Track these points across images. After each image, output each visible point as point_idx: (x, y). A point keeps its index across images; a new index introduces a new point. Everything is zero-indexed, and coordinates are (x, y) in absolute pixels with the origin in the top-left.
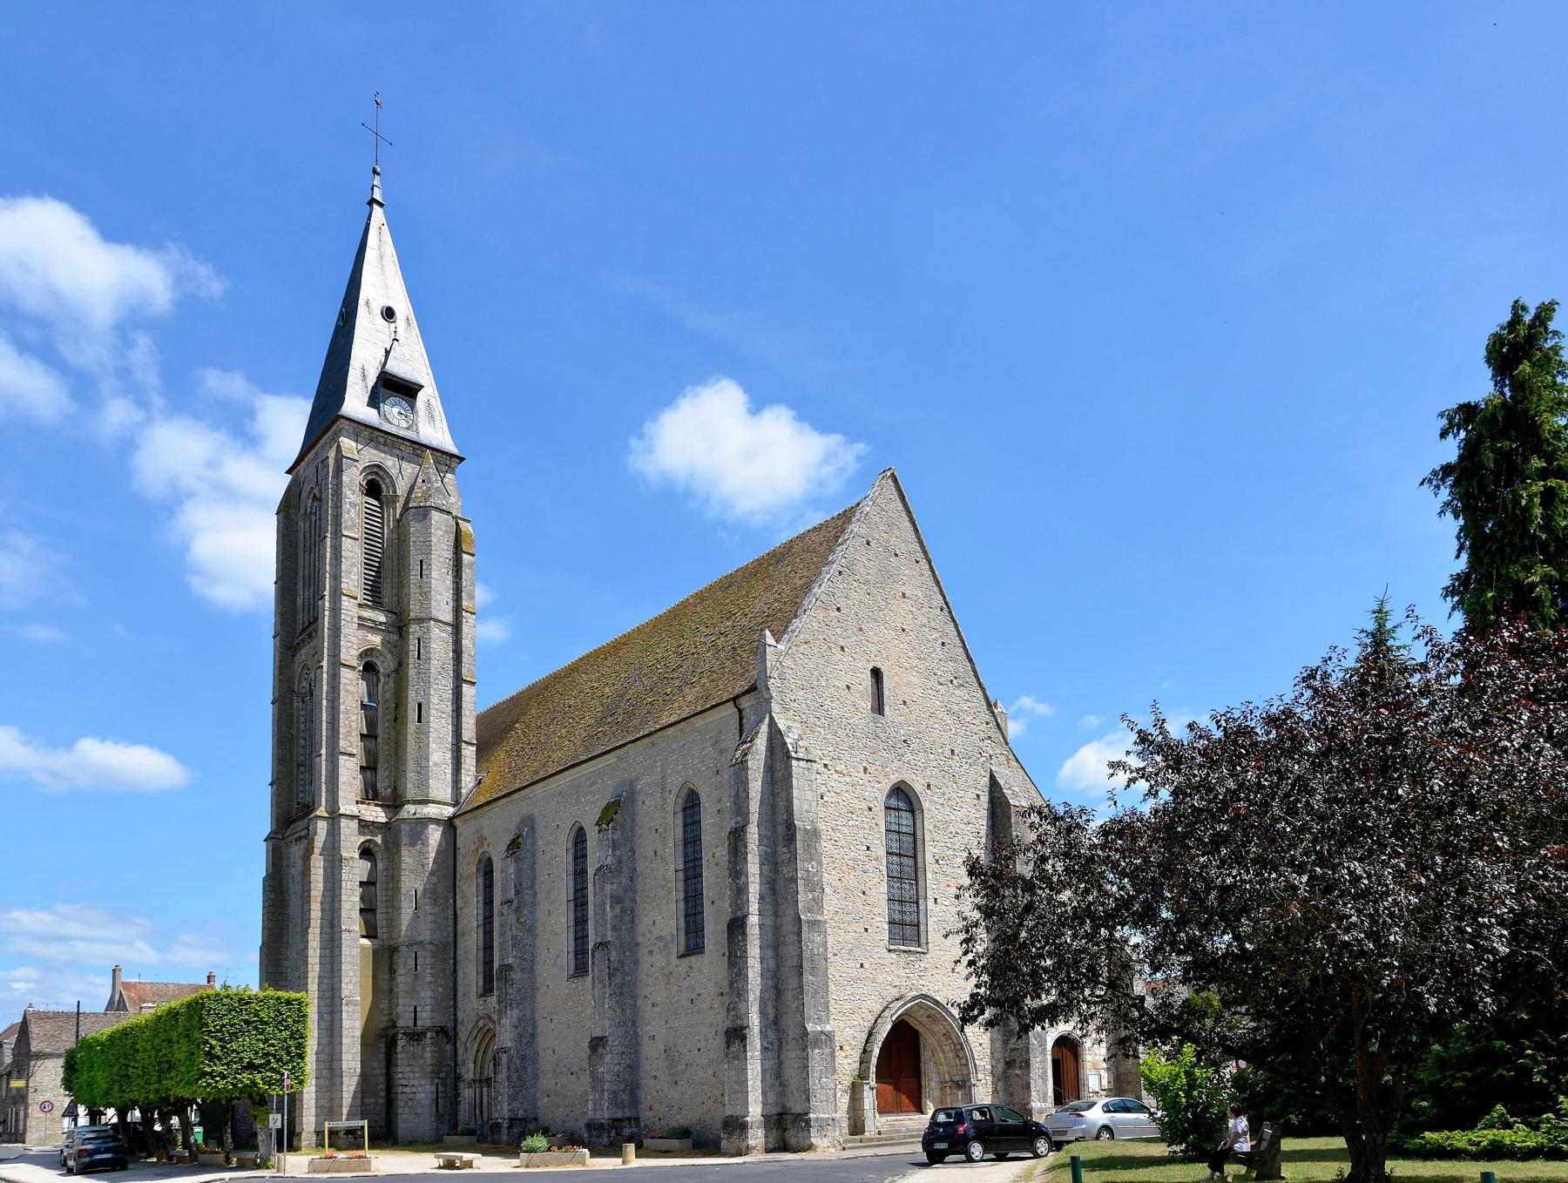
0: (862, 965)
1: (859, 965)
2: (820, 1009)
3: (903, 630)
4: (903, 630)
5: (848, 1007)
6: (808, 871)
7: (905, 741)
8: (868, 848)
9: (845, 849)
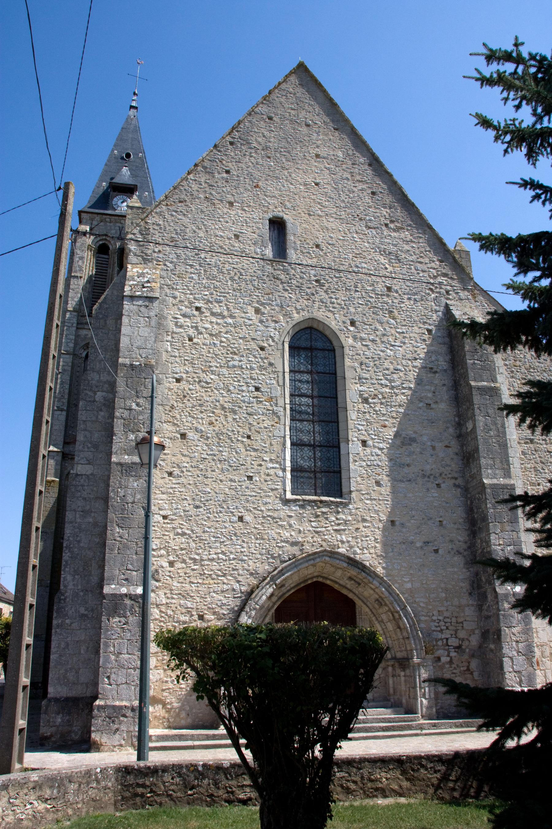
0: (241, 519)
1: (235, 519)
2: (130, 567)
3: (317, 184)
4: (317, 184)
5: (214, 568)
6: (130, 410)
7: (317, 281)
8: (257, 389)
9: (222, 391)
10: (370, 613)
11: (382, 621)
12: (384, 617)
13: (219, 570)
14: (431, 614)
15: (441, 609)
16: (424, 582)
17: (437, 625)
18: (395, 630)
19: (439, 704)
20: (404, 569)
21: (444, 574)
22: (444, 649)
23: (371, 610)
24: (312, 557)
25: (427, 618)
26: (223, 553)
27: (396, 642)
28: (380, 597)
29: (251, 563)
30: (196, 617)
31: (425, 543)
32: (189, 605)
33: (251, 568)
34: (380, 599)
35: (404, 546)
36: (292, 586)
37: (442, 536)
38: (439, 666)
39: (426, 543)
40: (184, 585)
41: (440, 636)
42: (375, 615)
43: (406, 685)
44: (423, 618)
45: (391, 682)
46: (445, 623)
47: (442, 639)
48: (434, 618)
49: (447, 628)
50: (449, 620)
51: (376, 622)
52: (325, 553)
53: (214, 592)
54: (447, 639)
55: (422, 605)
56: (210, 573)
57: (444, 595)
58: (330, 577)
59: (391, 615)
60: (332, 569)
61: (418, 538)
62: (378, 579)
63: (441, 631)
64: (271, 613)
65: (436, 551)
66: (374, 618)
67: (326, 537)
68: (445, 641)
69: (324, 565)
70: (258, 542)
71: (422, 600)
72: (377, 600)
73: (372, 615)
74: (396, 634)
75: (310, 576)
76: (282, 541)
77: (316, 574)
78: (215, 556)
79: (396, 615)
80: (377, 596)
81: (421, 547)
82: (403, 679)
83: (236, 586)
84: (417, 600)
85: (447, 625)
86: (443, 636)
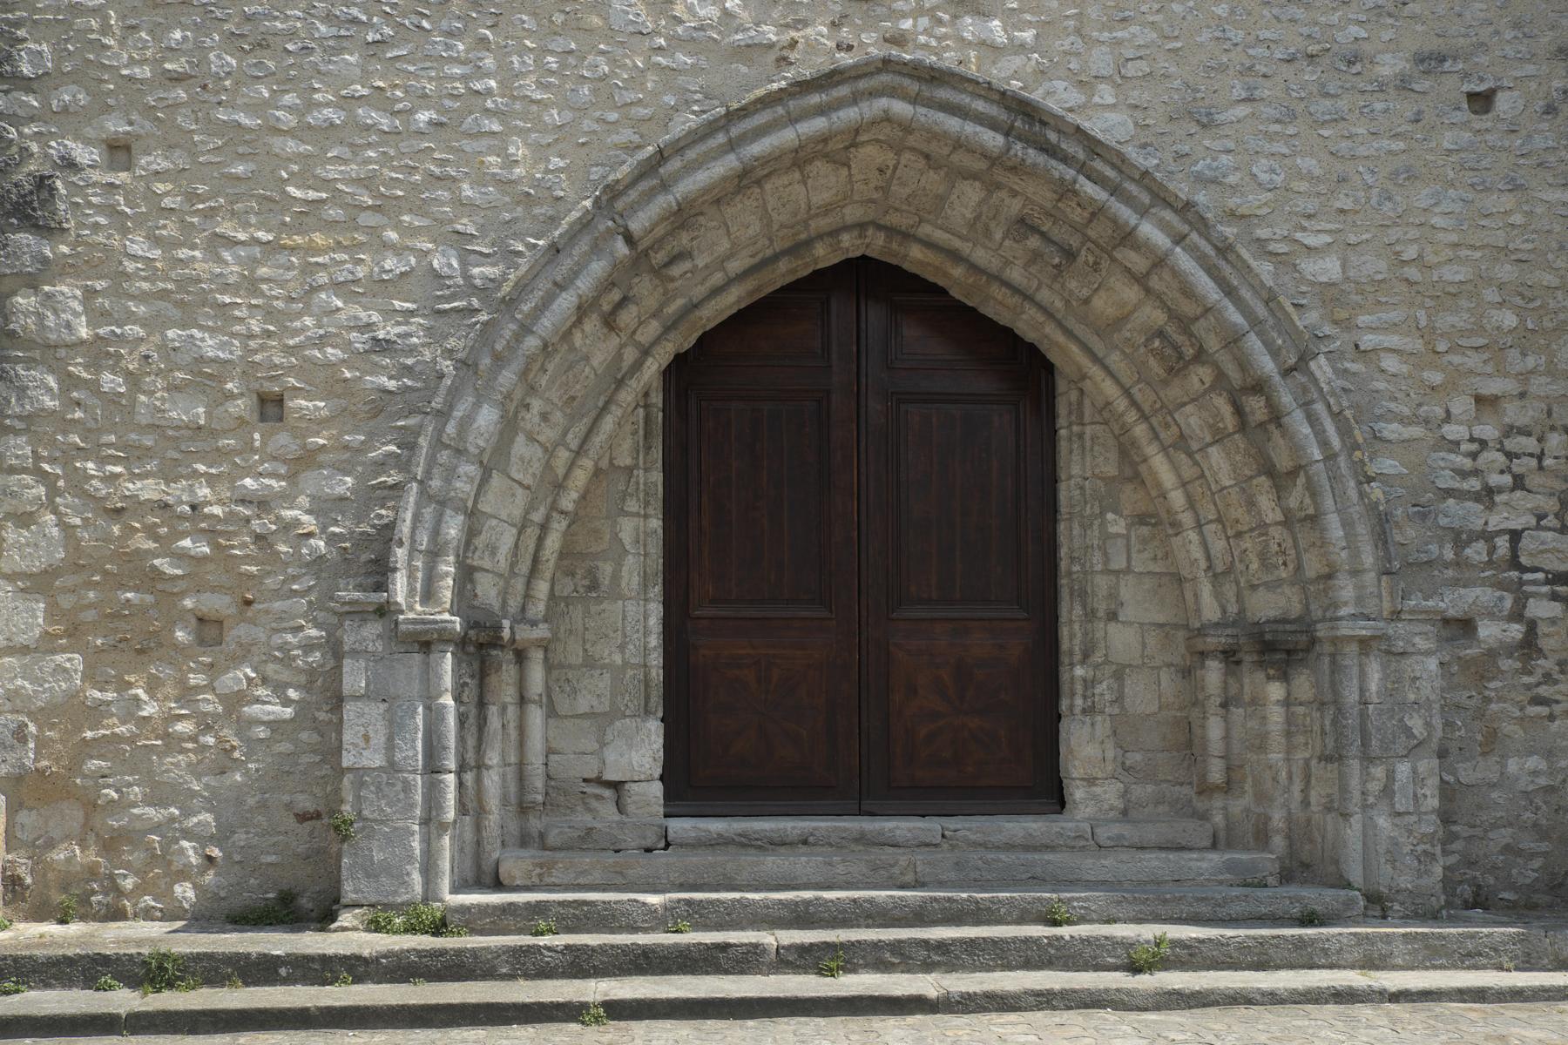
10: (1121, 404)
11: (1182, 443)
12: (1192, 420)
13: (358, 181)
14: (1439, 412)
15: (1492, 387)
16: (1411, 252)
17: (1467, 463)
18: (1244, 483)
19: (1458, 845)
20: (1303, 186)
21: (1517, 219)
22: (1500, 585)
23: (1127, 392)
24: (815, 99)
25: (1416, 431)
26: (379, 99)
27: (1247, 543)
28: (1173, 315)
29: (518, 149)
30: (241, 406)
31: (1420, 59)
32: (210, 346)
33: (519, 171)
34: (1171, 330)
35: (1310, 76)
36: (735, 266)
37: (1516, 25)
38: (1465, 664)
39: (1431, 62)
40: (183, 253)
41: (1473, 516)
42: (1144, 417)
43: (1290, 750)
44: (1391, 430)
45: (1215, 730)
46: (1510, 456)
47: (1488, 537)
48: (1453, 431)
49: (1519, 483)
50: (1530, 444)
51: (1151, 450)
52: (885, 78)
53: (337, 287)
54: (1515, 536)
55: (1390, 363)
56: (312, 195)
57: (1509, 320)
58: (926, 230)
59: (1226, 410)
60: (933, 181)
61: (1387, 35)
62: (1168, 215)
63: (1487, 495)
64: (627, 396)
65: (1481, 101)
66: (1140, 431)
67: (907, 24)
68: (1502, 543)
69: (889, 158)
70: (559, 44)
71: (1394, 340)
72: (1160, 334)
73: (1132, 416)
74: (1251, 504)
75: (822, 224)
76: (677, 42)
77: (852, 214)
78: (336, 117)
79: (1256, 407)
80: (1159, 317)
81: (1403, 84)
82: (1276, 716)
83: (445, 261)
84: (1368, 341)
85: (1519, 466)
86: (1496, 521)
